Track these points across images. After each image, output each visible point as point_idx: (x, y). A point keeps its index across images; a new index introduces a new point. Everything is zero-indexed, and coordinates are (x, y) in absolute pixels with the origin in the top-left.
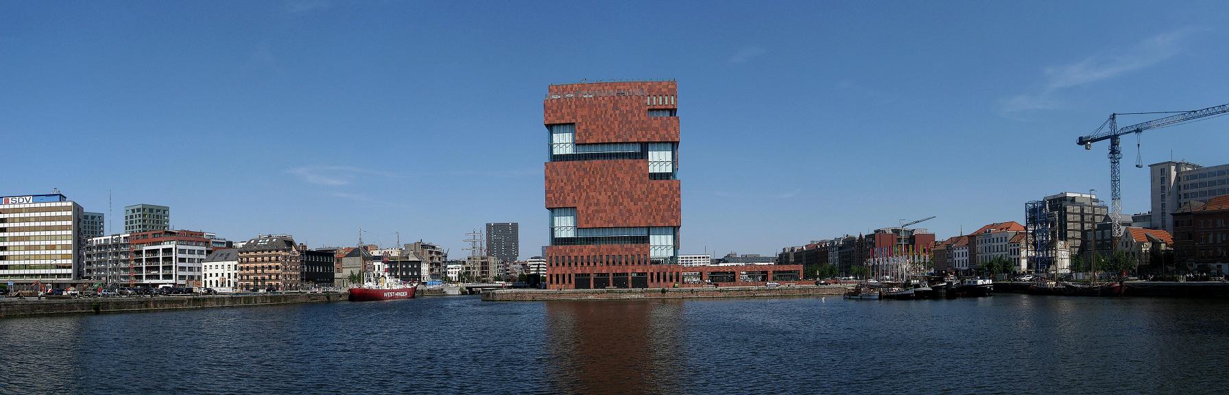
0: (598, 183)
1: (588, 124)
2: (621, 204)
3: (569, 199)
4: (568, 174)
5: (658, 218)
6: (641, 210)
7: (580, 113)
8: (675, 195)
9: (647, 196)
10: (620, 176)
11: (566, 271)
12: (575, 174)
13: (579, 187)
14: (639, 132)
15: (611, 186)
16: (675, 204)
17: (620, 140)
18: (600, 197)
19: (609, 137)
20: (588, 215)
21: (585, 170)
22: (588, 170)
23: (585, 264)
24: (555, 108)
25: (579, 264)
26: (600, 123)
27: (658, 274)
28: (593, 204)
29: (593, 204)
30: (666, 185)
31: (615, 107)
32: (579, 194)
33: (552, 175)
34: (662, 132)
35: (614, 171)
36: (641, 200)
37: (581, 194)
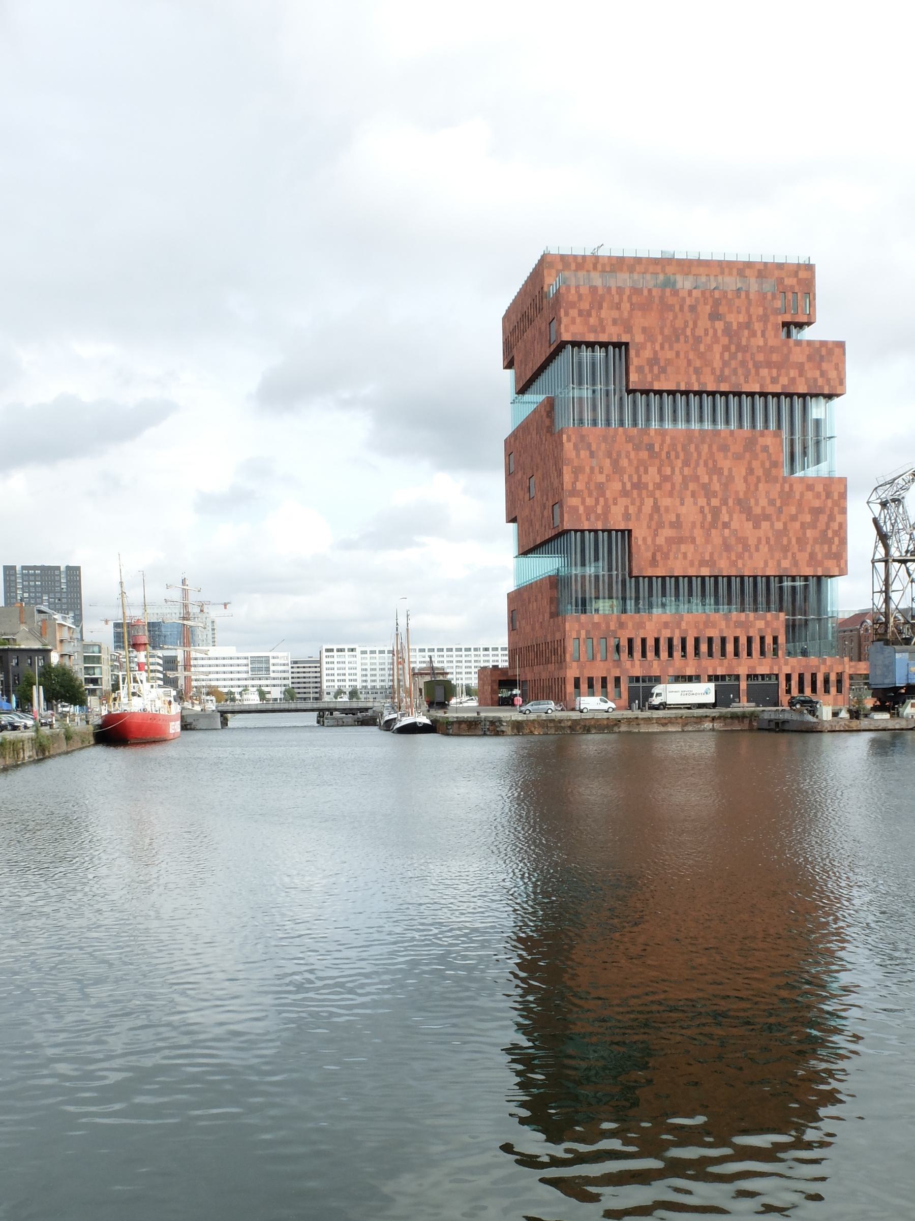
0: (678, 479)
1: (658, 348)
2: (726, 525)
3: (614, 509)
4: (614, 455)
5: (803, 557)
6: (768, 539)
7: (639, 321)
8: (836, 509)
9: (780, 511)
10: (725, 464)
11: (608, 670)
12: (628, 456)
13: (638, 486)
14: (764, 372)
15: (705, 487)
16: (836, 528)
17: (724, 387)
18: (683, 510)
19: (702, 380)
20: (659, 548)
21: (650, 447)
22: (657, 449)
23: (650, 654)
24: (585, 306)
25: (637, 654)
26: (680, 346)
27: (801, 677)
28: (667, 524)
29: (667, 524)
30: (819, 488)
31: (715, 316)
32: (638, 504)
33: (578, 455)
34: (812, 373)
35: (711, 454)
36: (767, 517)
37: (642, 503)
